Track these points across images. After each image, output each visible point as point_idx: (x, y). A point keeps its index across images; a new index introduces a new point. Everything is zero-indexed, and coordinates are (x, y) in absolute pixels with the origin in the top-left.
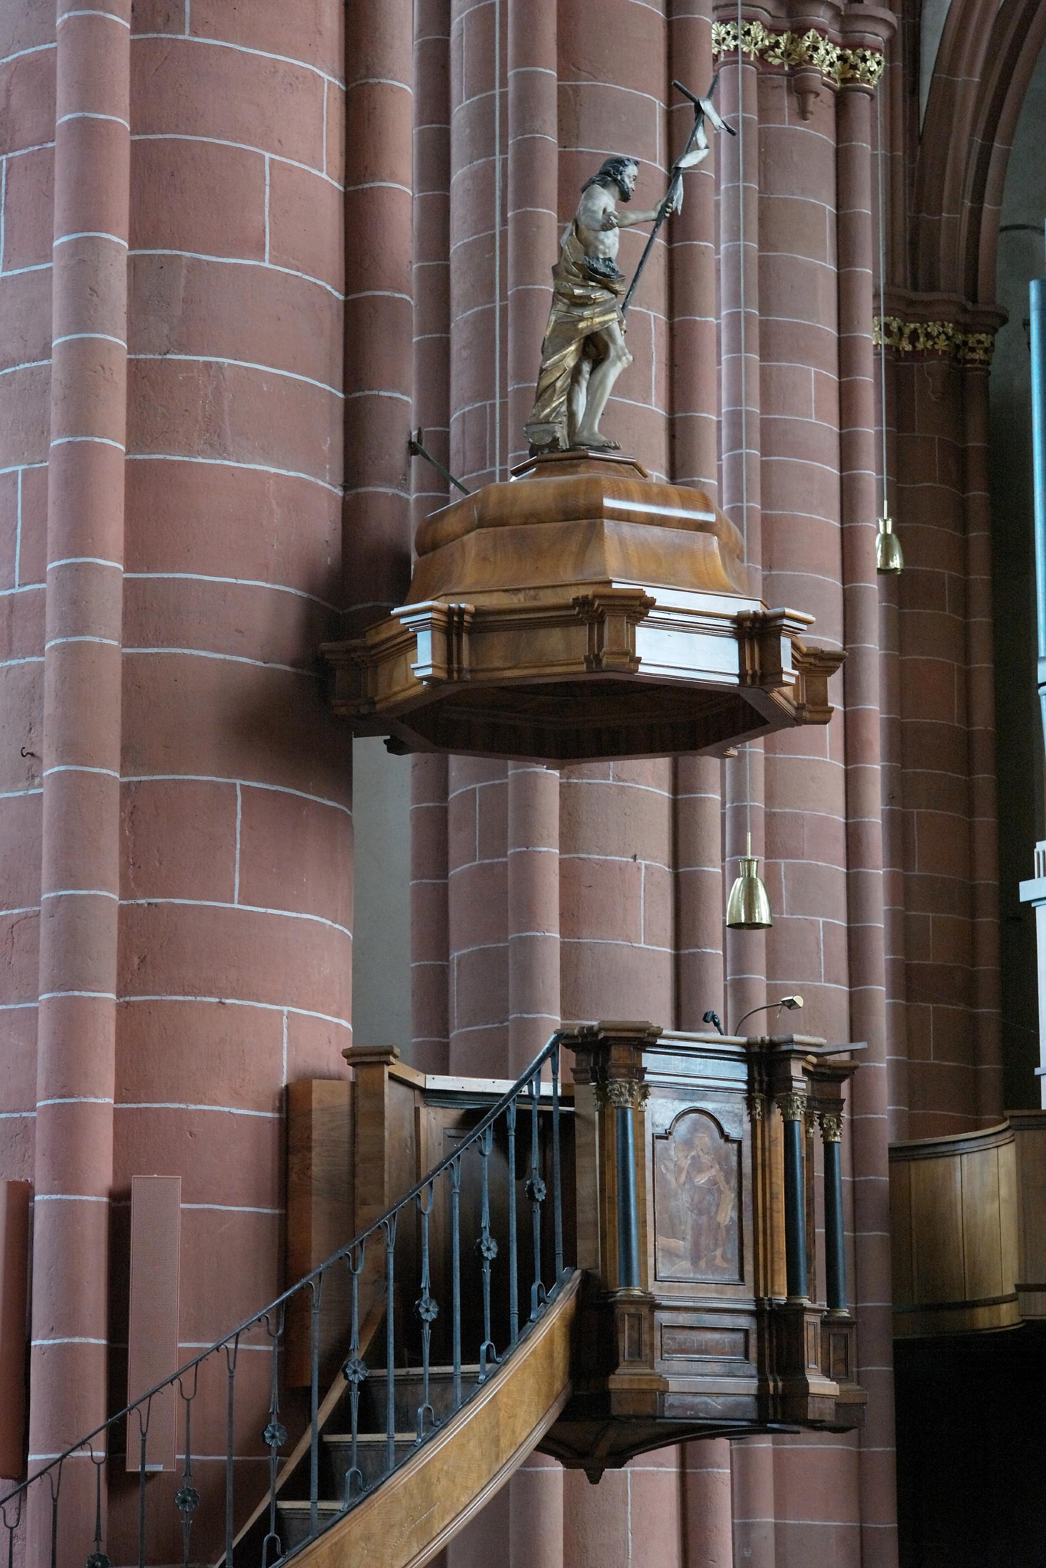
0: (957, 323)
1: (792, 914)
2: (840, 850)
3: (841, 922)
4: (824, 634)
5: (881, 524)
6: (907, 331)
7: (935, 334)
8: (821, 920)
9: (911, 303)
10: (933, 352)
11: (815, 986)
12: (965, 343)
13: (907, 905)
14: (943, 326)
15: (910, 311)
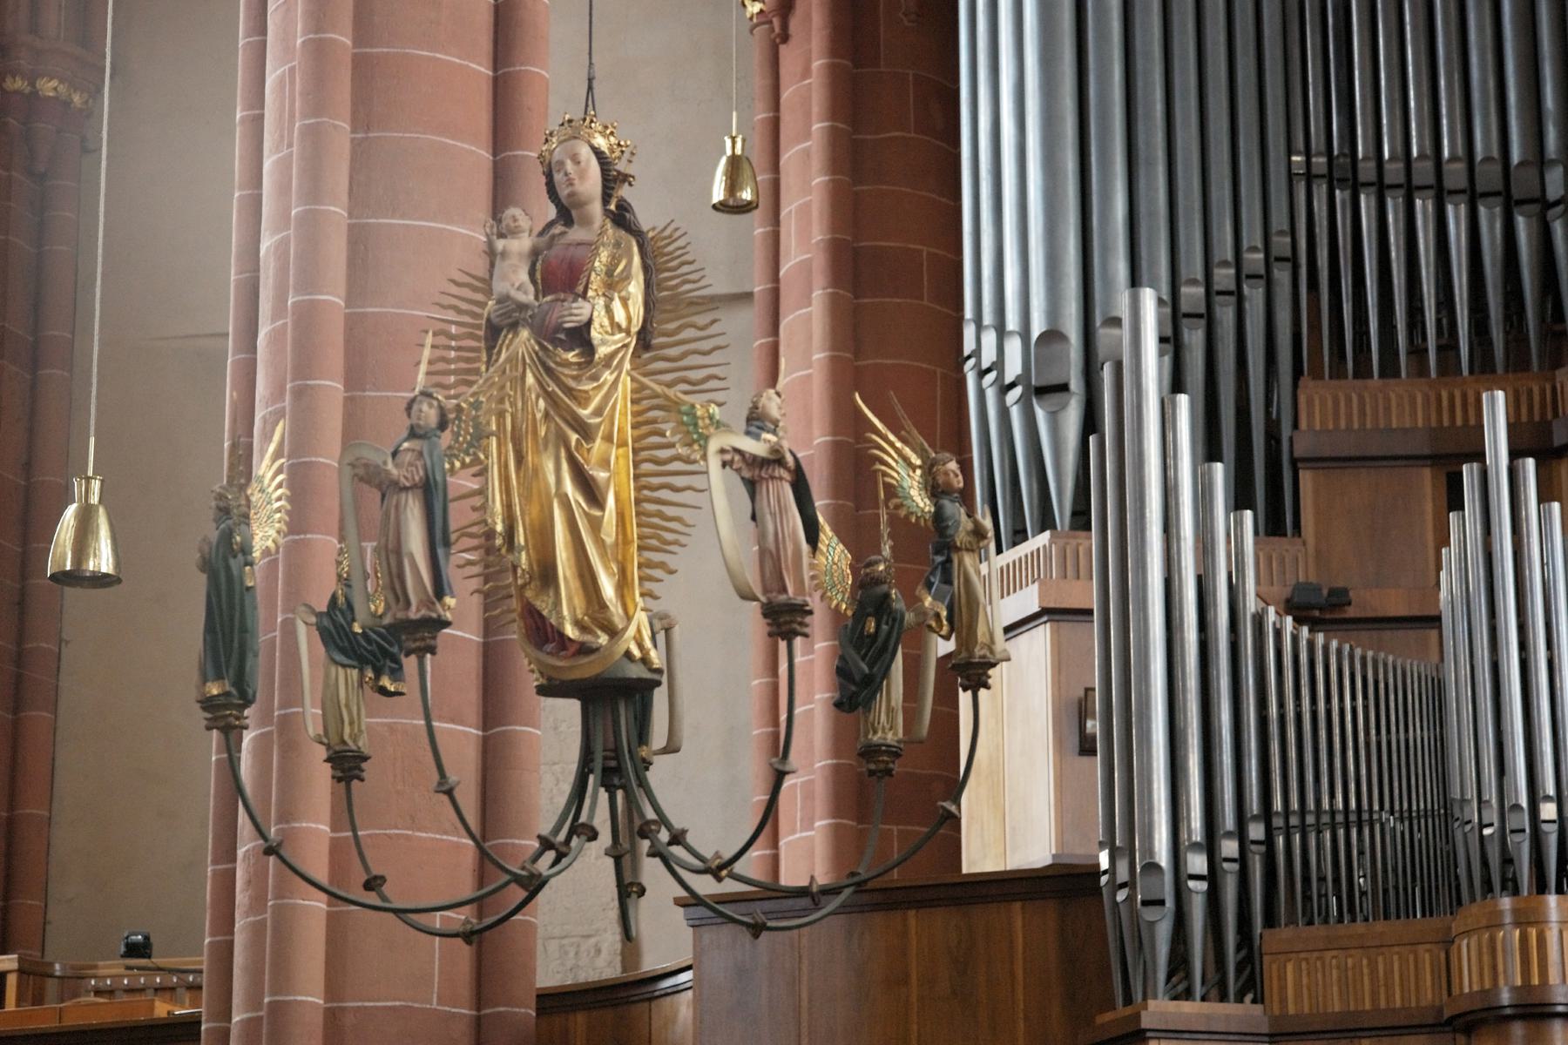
5: (728, 142)
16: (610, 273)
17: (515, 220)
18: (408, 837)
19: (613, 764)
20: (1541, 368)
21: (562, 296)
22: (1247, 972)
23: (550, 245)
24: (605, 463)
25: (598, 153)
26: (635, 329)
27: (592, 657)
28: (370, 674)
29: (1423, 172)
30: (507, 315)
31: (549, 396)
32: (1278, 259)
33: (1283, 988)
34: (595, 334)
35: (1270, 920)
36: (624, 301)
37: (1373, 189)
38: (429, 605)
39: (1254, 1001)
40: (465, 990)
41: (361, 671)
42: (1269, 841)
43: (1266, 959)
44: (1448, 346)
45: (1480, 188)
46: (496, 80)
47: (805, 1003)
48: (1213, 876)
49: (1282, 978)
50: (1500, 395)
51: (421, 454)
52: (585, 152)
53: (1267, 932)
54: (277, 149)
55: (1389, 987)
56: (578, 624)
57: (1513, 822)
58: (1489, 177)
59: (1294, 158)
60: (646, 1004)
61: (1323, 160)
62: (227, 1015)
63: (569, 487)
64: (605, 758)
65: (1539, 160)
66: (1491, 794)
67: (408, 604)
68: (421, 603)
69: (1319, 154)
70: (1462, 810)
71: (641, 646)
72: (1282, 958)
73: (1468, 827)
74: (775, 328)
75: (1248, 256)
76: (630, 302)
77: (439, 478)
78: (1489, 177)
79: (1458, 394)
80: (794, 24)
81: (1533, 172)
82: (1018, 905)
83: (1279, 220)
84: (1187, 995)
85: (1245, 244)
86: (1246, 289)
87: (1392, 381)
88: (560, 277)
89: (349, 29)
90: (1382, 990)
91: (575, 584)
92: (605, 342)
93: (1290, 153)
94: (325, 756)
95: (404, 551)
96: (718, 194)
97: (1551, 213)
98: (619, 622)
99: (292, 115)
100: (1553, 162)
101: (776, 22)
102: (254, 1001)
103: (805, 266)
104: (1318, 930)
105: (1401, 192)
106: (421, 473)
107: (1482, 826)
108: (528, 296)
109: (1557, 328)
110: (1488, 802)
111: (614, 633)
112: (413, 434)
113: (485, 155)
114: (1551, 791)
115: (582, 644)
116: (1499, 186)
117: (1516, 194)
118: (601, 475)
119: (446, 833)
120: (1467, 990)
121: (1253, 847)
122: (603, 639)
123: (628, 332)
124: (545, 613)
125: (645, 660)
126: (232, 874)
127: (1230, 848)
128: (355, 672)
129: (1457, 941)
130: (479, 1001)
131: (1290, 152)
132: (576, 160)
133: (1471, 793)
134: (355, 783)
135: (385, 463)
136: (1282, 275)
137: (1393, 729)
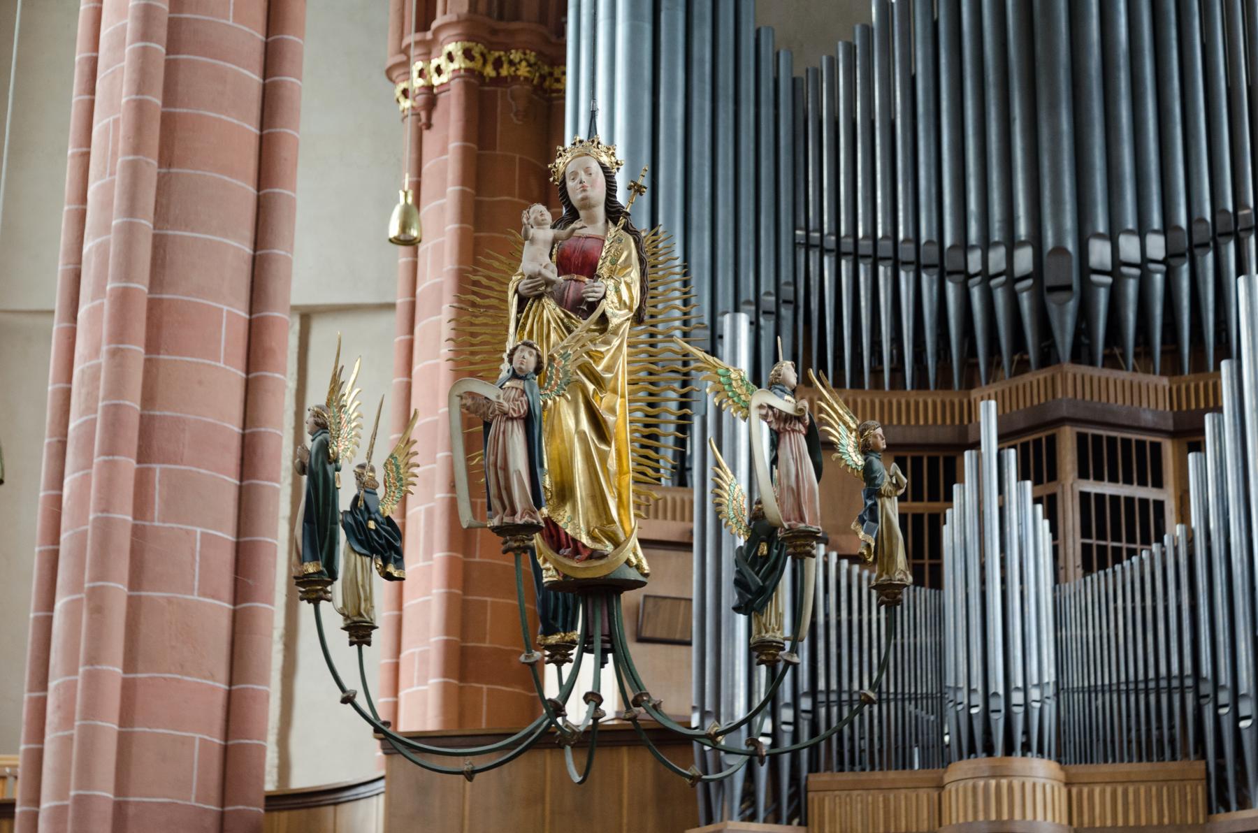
0: (540, 54)
1: (164, 521)
2: (232, 459)
3: (229, 536)
4: (226, 236)
5: (402, 194)
6: (491, 59)
7: (517, 60)
8: (199, 530)
9: (494, 32)
10: (515, 78)
11: (186, 600)
12: (551, 74)
13: (466, 587)
14: (525, 54)
15: (494, 39)
18: (179, 681)
19: (608, 646)
20: (960, 388)
22: (795, 803)
24: (612, 411)
27: (602, 562)
29: (885, 248)
30: (535, 288)
32: (786, 302)
33: (821, 815)
35: (814, 767)
36: (628, 286)
37: (851, 258)
39: (800, 824)
40: (214, 792)
42: (814, 711)
43: (810, 795)
44: (898, 368)
45: (923, 261)
46: (261, 138)
47: (467, 813)
48: (775, 735)
49: (821, 808)
50: (993, 403)
53: (812, 777)
54: (101, 176)
55: (897, 818)
57: (993, 704)
58: (929, 255)
59: (798, 232)
60: (331, 808)
61: (817, 235)
62: (36, 801)
63: (585, 425)
64: (603, 642)
65: (963, 245)
66: (977, 684)
69: (814, 231)
70: (955, 695)
71: (635, 555)
72: (821, 794)
73: (960, 707)
74: (411, 330)
75: (764, 298)
78: (929, 255)
79: (903, 402)
80: (436, 117)
81: (959, 254)
82: (625, 750)
83: (785, 275)
84: (753, 818)
85: (763, 290)
86: (762, 321)
87: (859, 391)
89: (161, 96)
90: (892, 820)
93: (795, 228)
94: (342, 625)
96: (394, 230)
97: (971, 282)
98: (622, 538)
99: (115, 154)
100: (973, 247)
101: (423, 115)
102: (61, 792)
103: (438, 287)
104: (847, 776)
105: (870, 261)
107: (970, 707)
108: (551, 273)
109: (972, 361)
110: (975, 690)
111: (617, 544)
113: (252, 190)
114: (1020, 684)
115: (594, 551)
116: (935, 260)
117: (948, 266)
118: (610, 419)
119: (205, 678)
120: (954, 822)
121: (804, 715)
122: (609, 548)
123: (630, 309)
124: (561, 524)
125: (638, 567)
126: (43, 701)
127: (787, 714)
129: (948, 787)
130: (223, 801)
131: (795, 228)
132: (588, 171)
133: (962, 683)
134: (364, 647)
136: (786, 312)
137: (906, 635)
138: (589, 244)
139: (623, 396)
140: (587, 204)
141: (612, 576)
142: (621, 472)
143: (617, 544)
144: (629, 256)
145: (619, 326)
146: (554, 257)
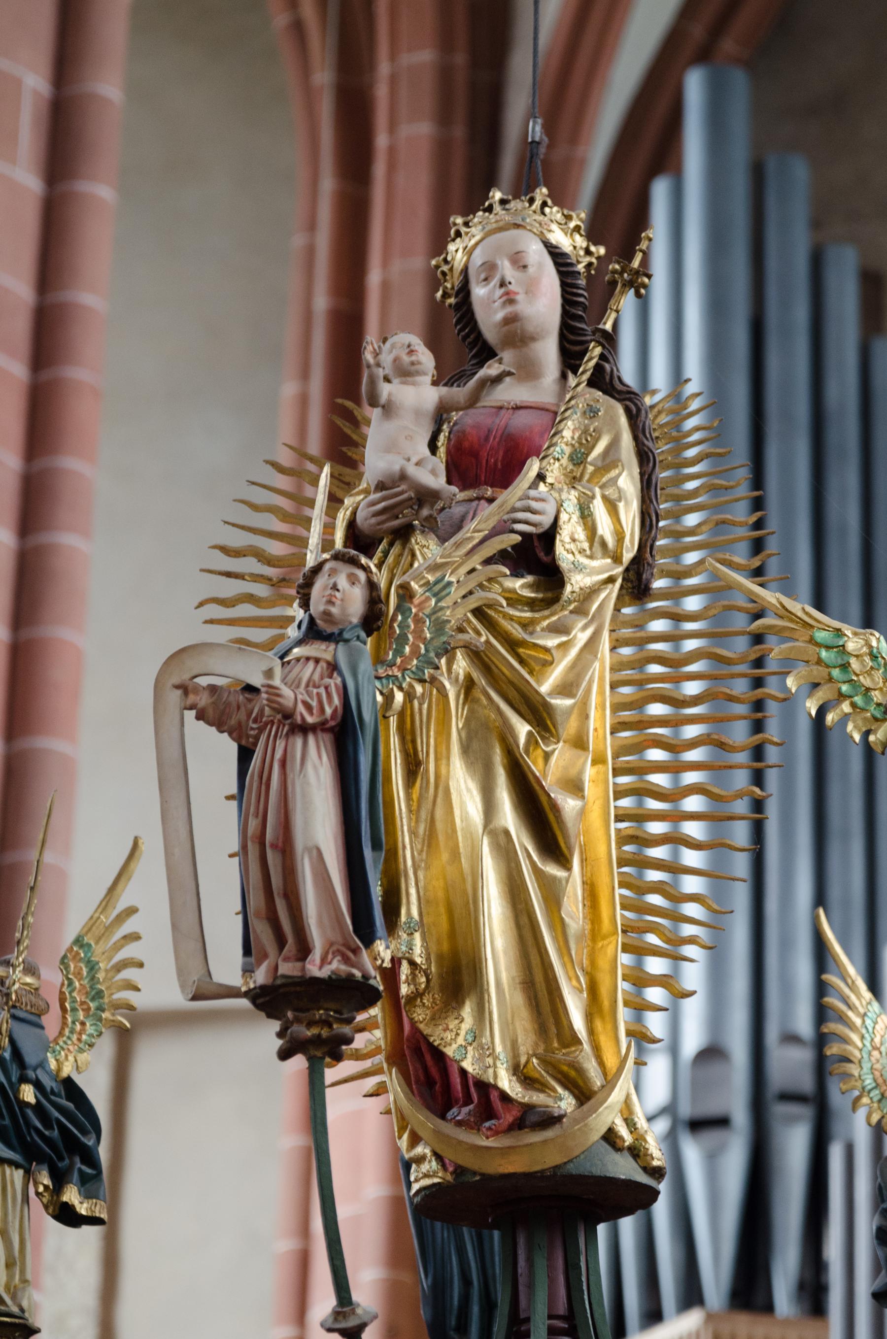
16: (578, 458)
17: (411, 352)
21: (489, 492)
23: (473, 401)
25: (556, 254)
26: (628, 556)
27: (549, 1134)
28: (45, 1179)
31: (476, 655)
34: (565, 552)
36: (612, 506)
38: (348, 953)
41: (28, 1173)
51: (333, 667)
52: (535, 252)
56: (518, 1071)
63: (508, 816)
67: (304, 950)
68: (335, 949)
76: (621, 506)
77: (367, 716)
88: (486, 461)
91: (517, 999)
92: (584, 569)
95: (299, 843)
98: (597, 1081)
106: (336, 701)
111: (584, 1095)
112: (313, 632)
115: (528, 1108)
118: (569, 805)
122: (566, 1103)
124: (450, 1051)
125: (636, 1152)
128: (19, 1174)
132: (519, 262)
135: (269, 673)
138: (521, 421)
139: (599, 760)
140: (517, 334)
141: (572, 1169)
142: (595, 933)
143: (584, 1095)
144: (614, 444)
145: (589, 594)
146: (442, 451)
